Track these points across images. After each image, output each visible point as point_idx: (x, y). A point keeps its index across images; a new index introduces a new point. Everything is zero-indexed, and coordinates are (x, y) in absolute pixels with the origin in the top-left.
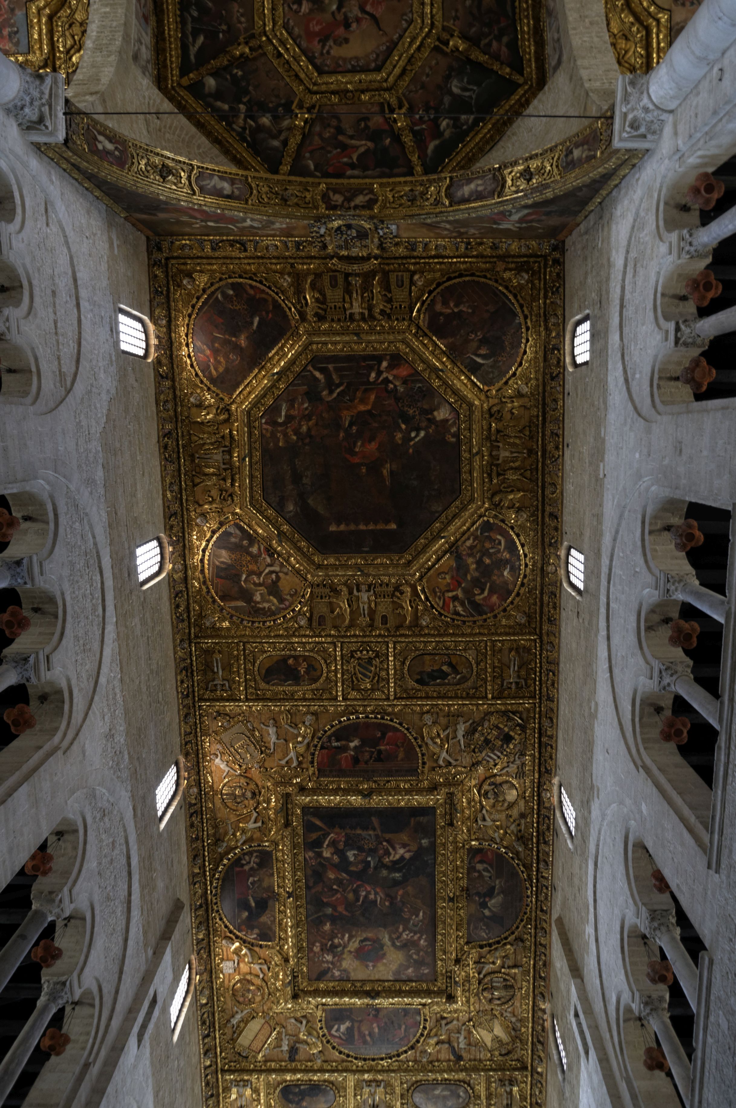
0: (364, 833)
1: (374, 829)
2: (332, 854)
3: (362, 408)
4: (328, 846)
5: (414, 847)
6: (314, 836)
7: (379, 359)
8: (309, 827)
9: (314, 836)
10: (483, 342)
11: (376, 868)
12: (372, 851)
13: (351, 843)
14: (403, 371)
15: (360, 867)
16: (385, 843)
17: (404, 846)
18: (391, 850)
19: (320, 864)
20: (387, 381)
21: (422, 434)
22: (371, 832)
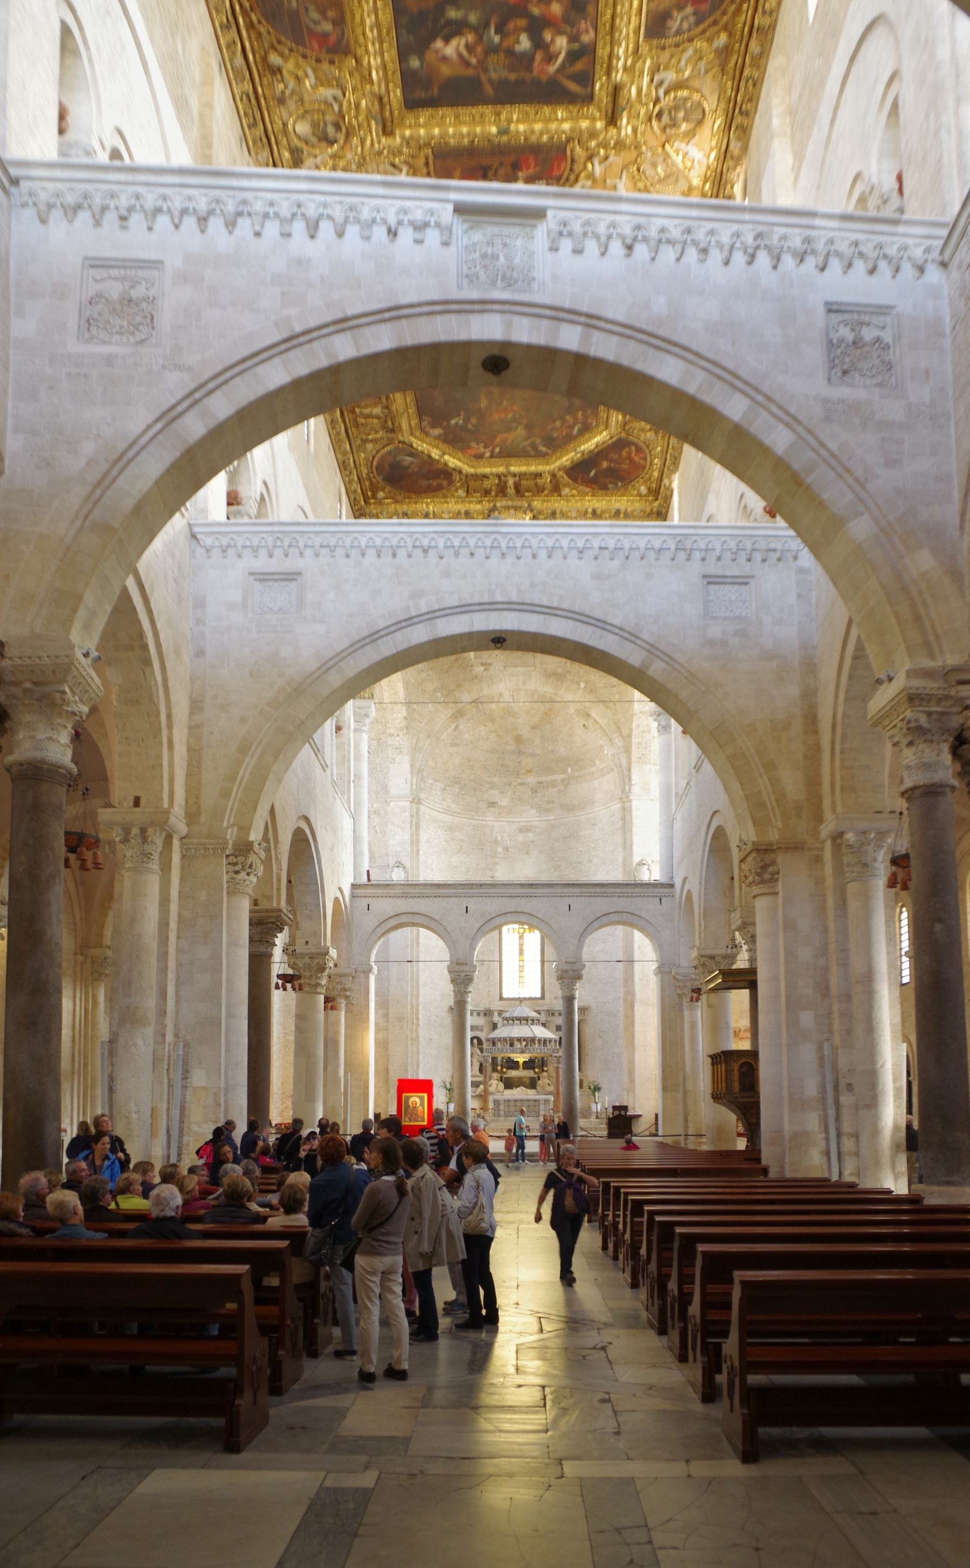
0: (504, 74)
1: (491, 81)
2: (553, 41)
3: (506, 435)
4: (559, 53)
5: (430, 56)
6: (579, 66)
7: (492, 456)
8: (586, 79)
9: (579, 66)
10: (409, 467)
11: (487, 25)
12: (492, 50)
13: (525, 61)
14: (471, 452)
15: (511, 26)
16: (474, 61)
17: (445, 59)
18: (465, 53)
19: (572, 24)
20: (485, 447)
21: (453, 422)
22: (494, 75)
